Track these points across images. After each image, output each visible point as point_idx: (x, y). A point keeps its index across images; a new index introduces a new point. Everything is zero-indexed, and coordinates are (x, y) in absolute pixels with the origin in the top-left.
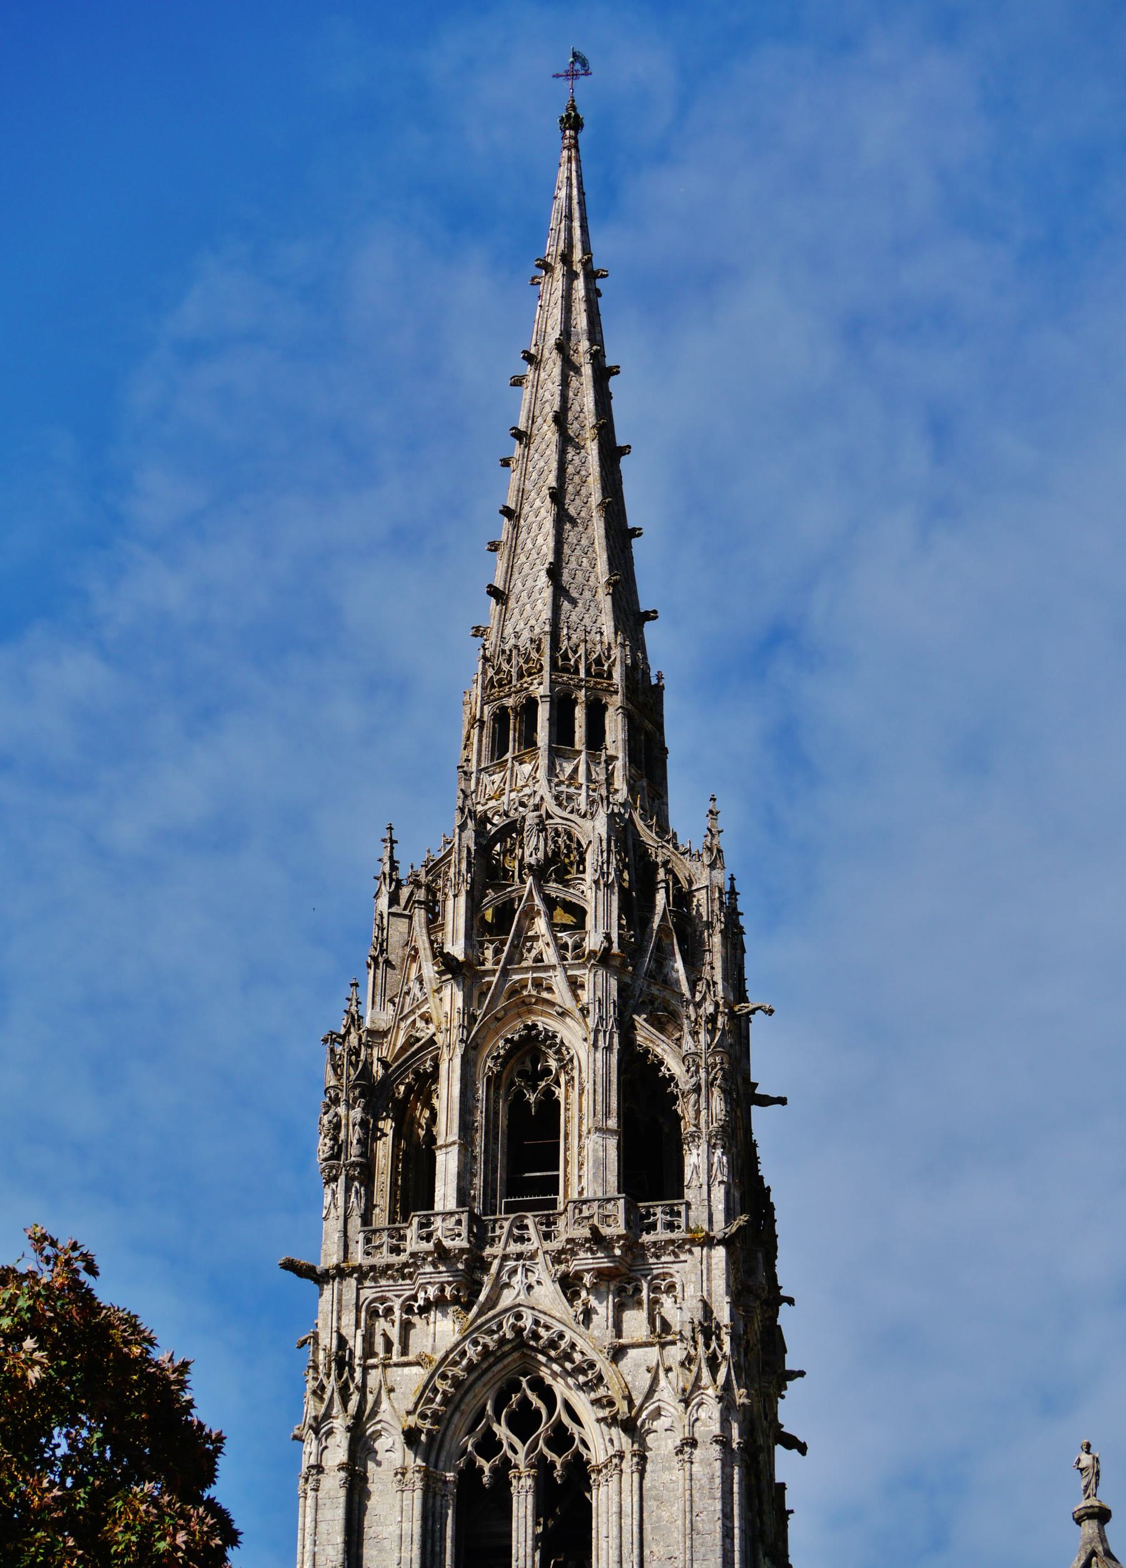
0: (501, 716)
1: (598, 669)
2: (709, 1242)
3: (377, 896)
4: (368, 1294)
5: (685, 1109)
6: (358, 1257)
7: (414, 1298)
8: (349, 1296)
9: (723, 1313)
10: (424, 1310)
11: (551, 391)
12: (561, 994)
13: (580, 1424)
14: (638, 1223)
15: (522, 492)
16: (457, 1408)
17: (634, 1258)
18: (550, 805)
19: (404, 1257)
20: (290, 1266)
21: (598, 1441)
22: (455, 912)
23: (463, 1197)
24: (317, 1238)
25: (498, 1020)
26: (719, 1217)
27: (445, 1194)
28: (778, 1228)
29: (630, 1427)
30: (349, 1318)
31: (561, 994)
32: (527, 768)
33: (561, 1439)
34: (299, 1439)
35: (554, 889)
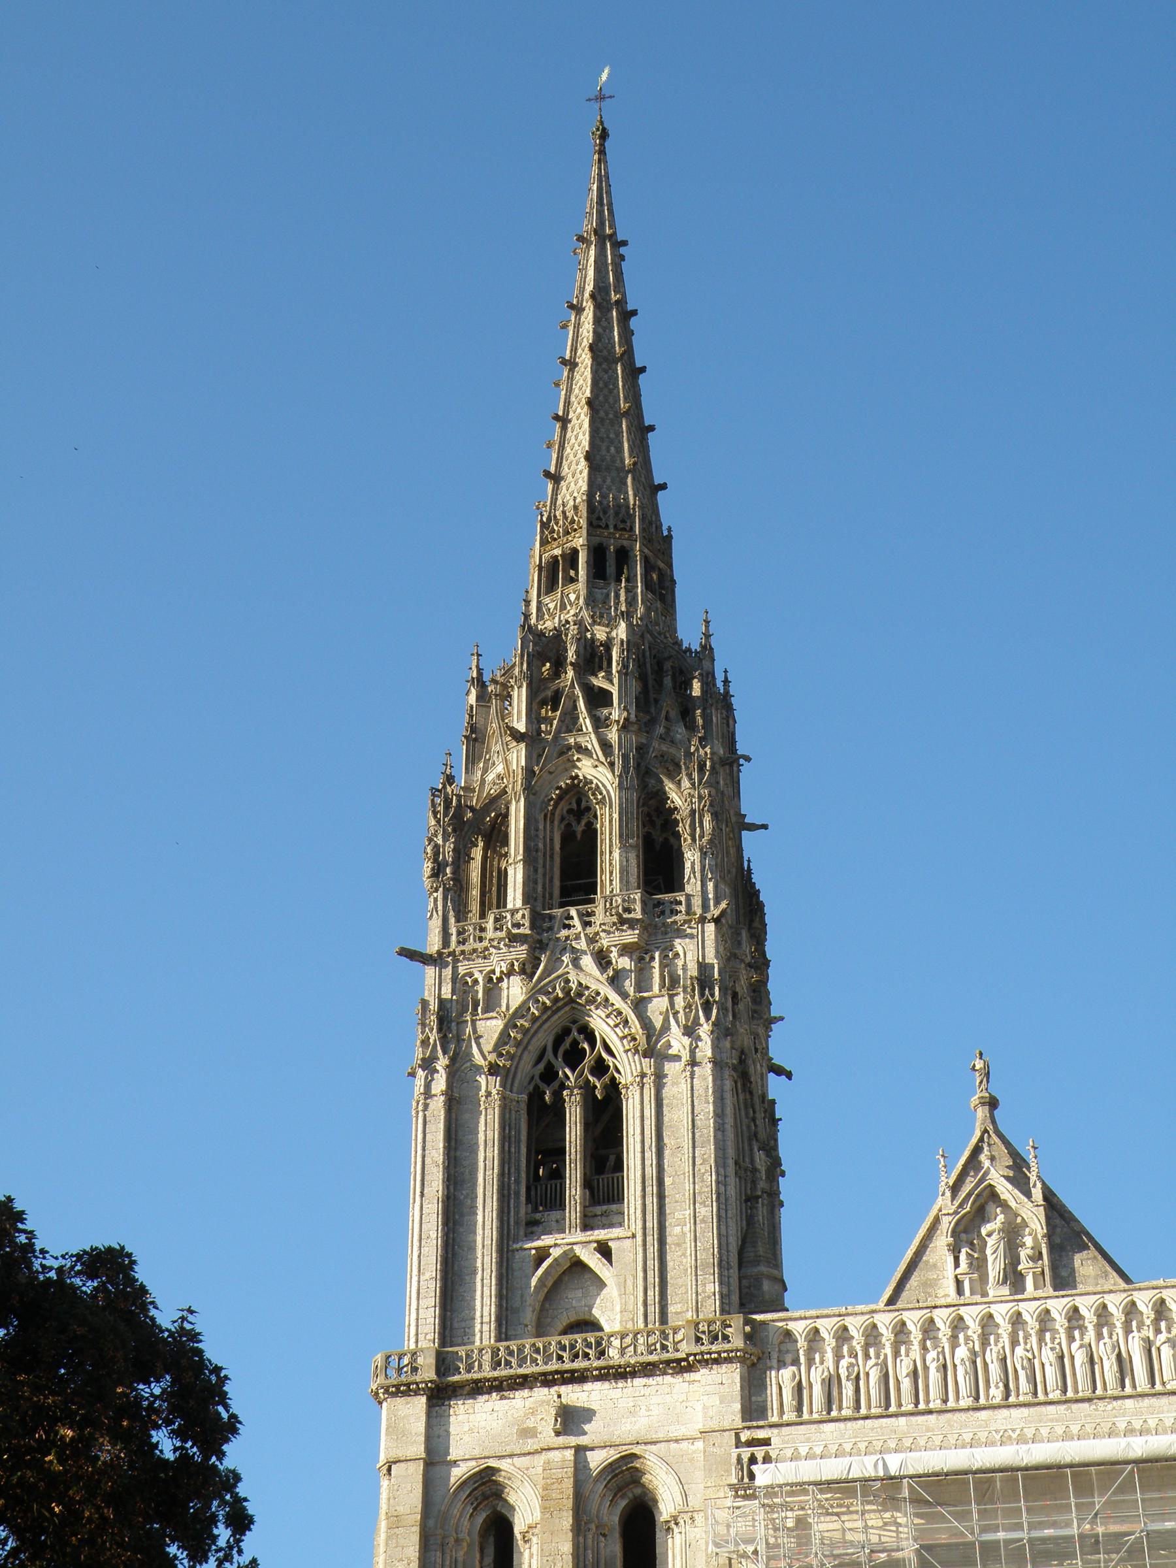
2: (702, 920)
3: (468, 693)
5: (684, 829)
7: (493, 972)
8: (448, 972)
13: (613, 1056)
15: (568, 403)
16: (525, 1048)
17: (650, 935)
19: (486, 943)
21: (628, 1067)
22: (520, 697)
23: (528, 898)
24: (425, 932)
25: (551, 773)
27: (515, 896)
28: (767, 919)
33: (600, 1068)
34: (412, 1075)
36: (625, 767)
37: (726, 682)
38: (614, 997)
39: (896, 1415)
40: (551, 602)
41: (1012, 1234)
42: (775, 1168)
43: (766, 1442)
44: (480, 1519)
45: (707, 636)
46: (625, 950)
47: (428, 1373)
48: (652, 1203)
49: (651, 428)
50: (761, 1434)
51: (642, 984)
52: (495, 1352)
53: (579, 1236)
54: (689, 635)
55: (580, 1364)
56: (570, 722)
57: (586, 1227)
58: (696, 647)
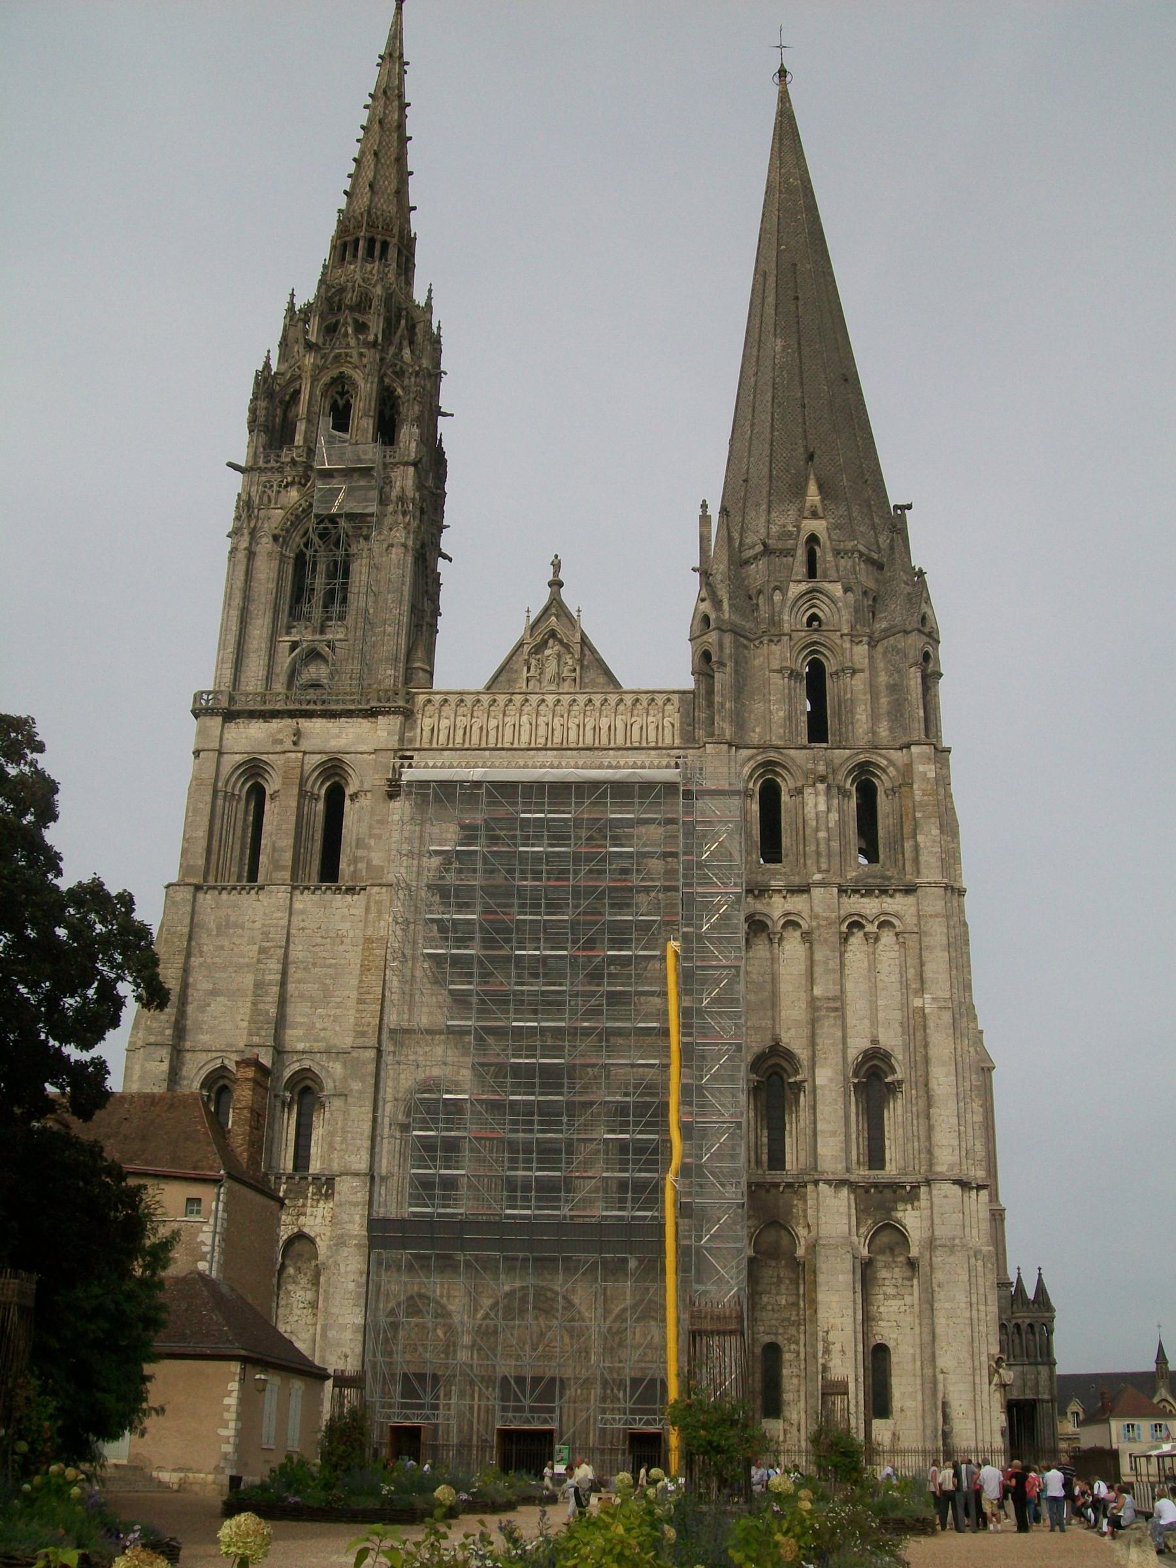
0: (345, 245)
1: (388, 229)
2: (406, 464)
4: (263, 479)
6: (261, 464)
10: (286, 486)
12: (355, 359)
18: (360, 281)
20: (230, 465)
22: (314, 325)
30: (254, 489)
31: (355, 359)
32: (352, 267)
37: (439, 328)
39: (484, 749)
42: (436, 612)
43: (411, 758)
44: (248, 785)
45: (430, 298)
50: (408, 754)
53: (318, 637)
54: (419, 297)
55: (312, 707)
57: (322, 633)
58: (422, 304)
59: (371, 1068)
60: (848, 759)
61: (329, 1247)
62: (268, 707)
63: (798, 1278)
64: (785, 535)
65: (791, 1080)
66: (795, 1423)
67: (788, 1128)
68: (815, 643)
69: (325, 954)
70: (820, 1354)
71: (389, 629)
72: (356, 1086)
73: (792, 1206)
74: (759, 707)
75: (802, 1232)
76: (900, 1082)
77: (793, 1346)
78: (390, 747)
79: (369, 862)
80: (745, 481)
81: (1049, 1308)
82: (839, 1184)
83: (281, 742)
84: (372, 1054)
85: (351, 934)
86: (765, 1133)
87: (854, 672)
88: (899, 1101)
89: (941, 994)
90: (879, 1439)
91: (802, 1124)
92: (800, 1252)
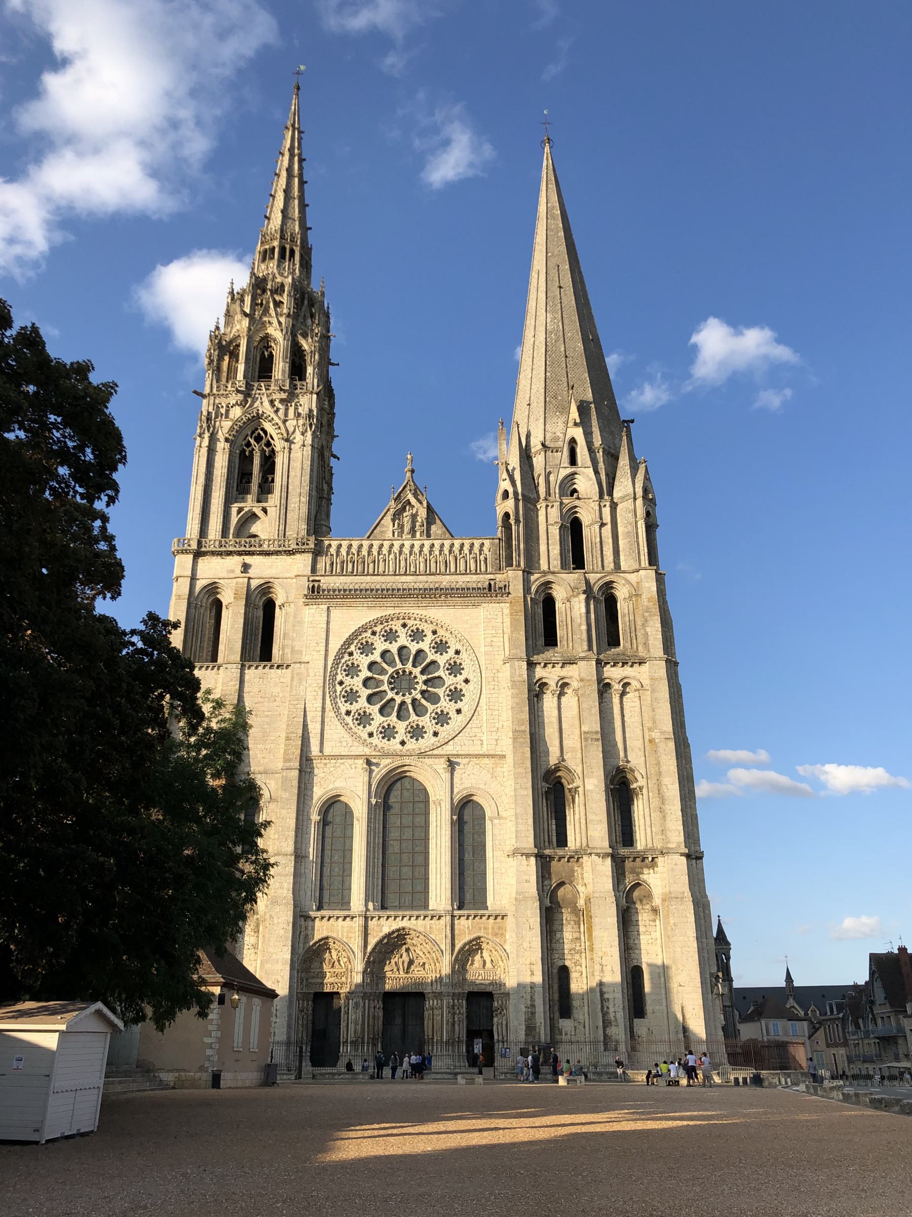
2: (312, 393)
4: (217, 402)
5: (308, 358)
8: (212, 402)
9: (315, 413)
11: (286, 163)
14: (293, 387)
15: (276, 191)
20: (195, 392)
22: (248, 300)
23: (245, 377)
26: (315, 387)
29: (287, 440)
33: (268, 444)
35: (277, 298)
36: (287, 332)
37: (328, 308)
38: (275, 418)
40: (263, 266)
41: (414, 517)
43: (319, 581)
46: (282, 401)
47: (194, 546)
48: (284, 494)
49: (308, 205)
50: (317, 578)
51: (286, 415)
52: (220, 542)
55: (252, 549)
56: (266, 311)
57: (259, 501)
59: (295, 783)
60: (599, 579)
61: (266, 906)
62: (223, 549)
63: (579, 920)
64: (556, 439)
65: (571, 786)
66: (582, 1021)
67: (568, 818)
68: (576, 507)
69: (263, 709)
70: (597, 973)
71: (303, 499)
72: (286, 795)
73: (573, 871)
74: (543, 548)
75: (581, 889)
76: (641, 788)
77: (578, 967)
78: (305, 573)
79: (293, 647)
80: (529, 405)
81: (728, 944)
82: (605, 856)
83: (233, 571)
84: (296, 773)
85: (281, 695)
86: (554, 822)
87: (603, 525)
88: (640, 801)
89: (665, 729)
90: (639, 1033)
91: (577, 817)
92: (581, 903)
